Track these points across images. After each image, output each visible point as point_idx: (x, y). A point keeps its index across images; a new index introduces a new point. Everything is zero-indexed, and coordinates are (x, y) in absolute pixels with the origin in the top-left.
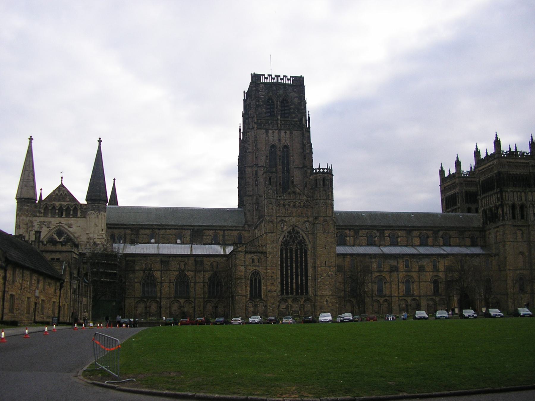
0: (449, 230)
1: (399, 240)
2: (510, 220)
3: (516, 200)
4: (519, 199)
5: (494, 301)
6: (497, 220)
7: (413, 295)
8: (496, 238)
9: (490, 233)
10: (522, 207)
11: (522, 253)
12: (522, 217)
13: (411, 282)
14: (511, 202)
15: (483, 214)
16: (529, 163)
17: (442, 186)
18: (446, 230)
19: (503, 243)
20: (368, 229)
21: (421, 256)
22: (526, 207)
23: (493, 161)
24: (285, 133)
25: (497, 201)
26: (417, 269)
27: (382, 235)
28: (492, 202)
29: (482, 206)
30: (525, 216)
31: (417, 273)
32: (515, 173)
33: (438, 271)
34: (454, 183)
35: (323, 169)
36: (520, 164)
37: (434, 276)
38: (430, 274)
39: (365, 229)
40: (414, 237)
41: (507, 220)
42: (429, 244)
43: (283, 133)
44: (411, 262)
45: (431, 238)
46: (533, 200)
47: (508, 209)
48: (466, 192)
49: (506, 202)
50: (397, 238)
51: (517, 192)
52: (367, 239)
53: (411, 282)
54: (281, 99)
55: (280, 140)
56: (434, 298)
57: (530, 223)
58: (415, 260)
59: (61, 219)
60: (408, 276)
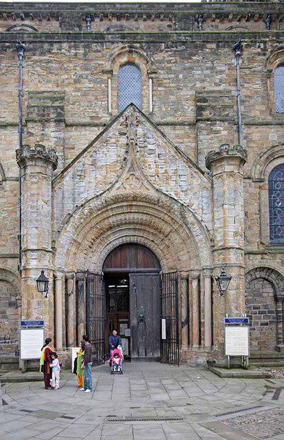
18: (119, 17)
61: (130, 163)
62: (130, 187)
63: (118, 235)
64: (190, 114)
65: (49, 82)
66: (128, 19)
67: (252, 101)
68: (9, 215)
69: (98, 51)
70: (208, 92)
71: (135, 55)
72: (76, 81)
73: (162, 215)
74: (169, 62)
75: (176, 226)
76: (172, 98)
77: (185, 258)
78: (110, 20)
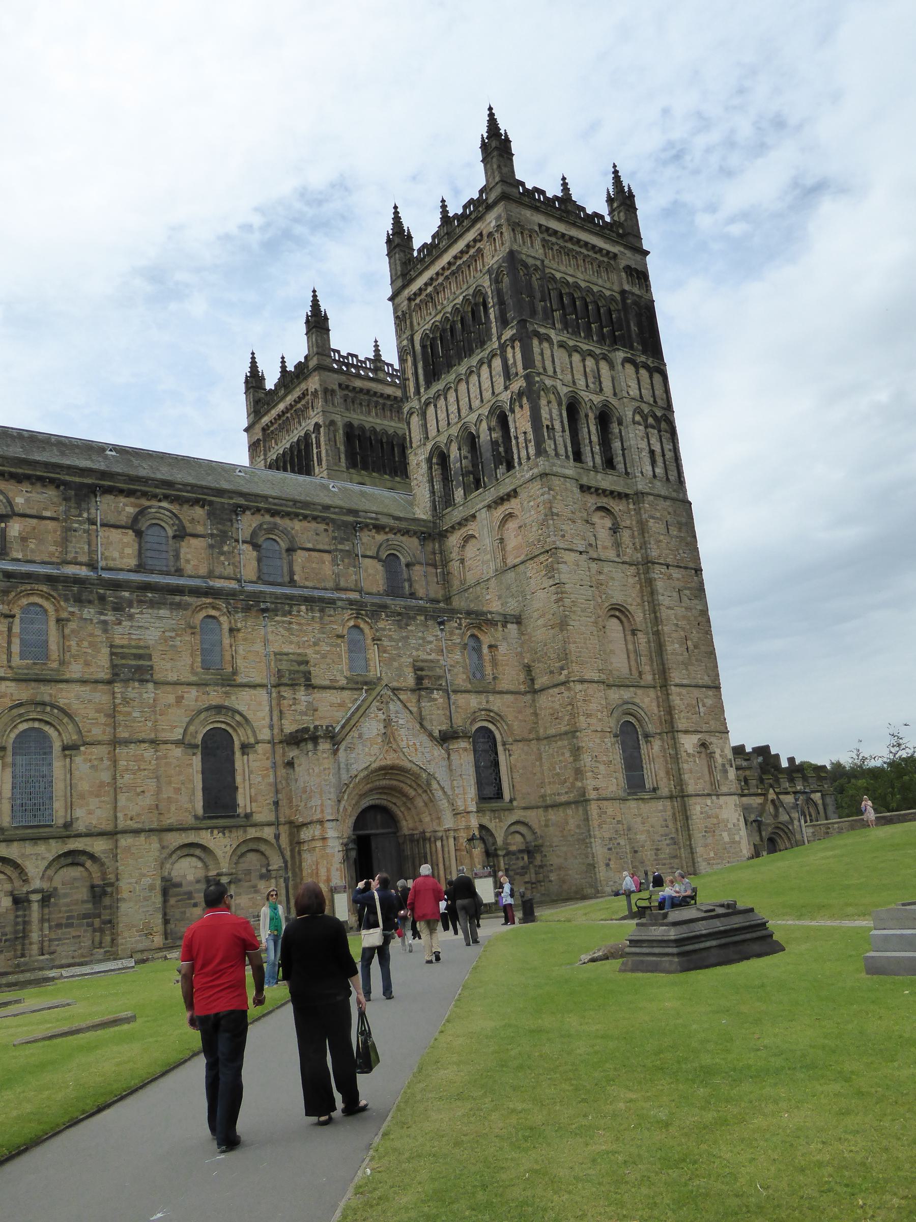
0: (288, 514)
1: (15, 528)
2: (567, 457)
3: (581, 383)
4: (591, 385)
5: (517, 843)
6: (502, 469)
7: (67, 831)
8: (503, 549)
9: (469, 538)
10: (604, 418)
11: (618, 612)
12: (609, 463)
13: (57, 746)
14: (563, 390)
15: (430, 468)
16: (615, 256)
17: (258, 428)
18: (274, 514)
19: (542, 558)
21: (126, 594)
22: (620, 423)
23: (478, 226)
25: (499, 387)
26: (101, 665)
28: (476, 403)
29: (427, 438)
30: (619, 459)
31: (101, 687)
32: (570, 280)
33: (229, 681)
34: (304, 395)
37: (207, 709)
38: (179, 699)
40: (103, 525)
41: (557, 455)
42: (189, 569)
44: (58, 620)
45: (194, 542)
46: (641, 397)
47: (555, 412)
48: (349, 426)
49: (549, 382)
51: (584, 355)
53: (57, 746)
56: (204, 838)
57: (641, 485)
58: (89, 612)
60: (44, 704)
61: (388, 736)
62: (390, 759)
63: (367, 799)
64: (410, 681)
65: (291, 643)
66: (283, 517)
67: (456, 670)
68: (263, 779)
69: (330, 616)
70: (423, 661)
71: (359, 621)
72: (315, 644)
73: (409, 782)
74: (390, 630)
75: (420, 791)
76: (395, 664)
77: (427, 819)
78: (263, 515)
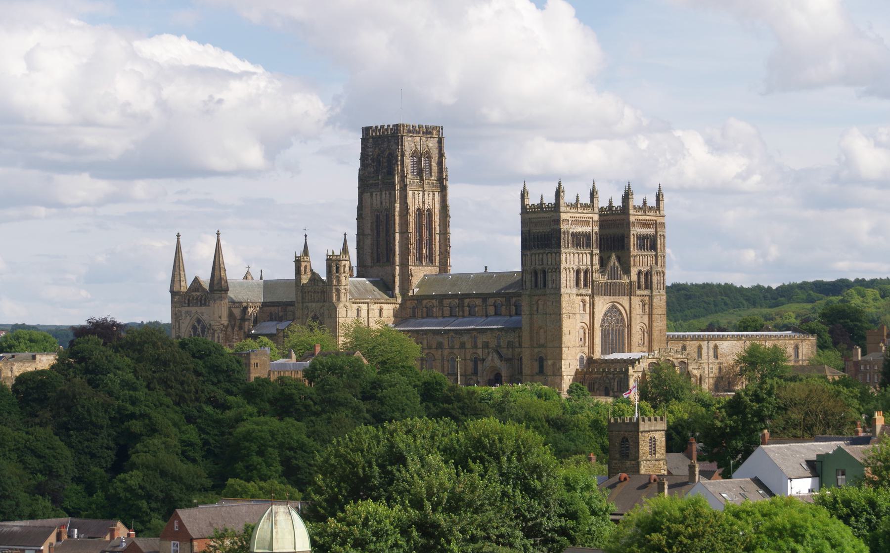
1: (476, 309)
10: (544, 272)
12: (545, 285)
14: (532, 268)
20: (450, 299)
24: (386, 194)
27: (461, 306)
35: (330, 256)
36: (543, 219)
39: (447, 299)
43: (384, 193)
45: (504, 307)
50: (475, 307)
52: (451, 310)
54: (387, 153)
55: (381, 203)
59: (196, 308)
61: (492, 360)
